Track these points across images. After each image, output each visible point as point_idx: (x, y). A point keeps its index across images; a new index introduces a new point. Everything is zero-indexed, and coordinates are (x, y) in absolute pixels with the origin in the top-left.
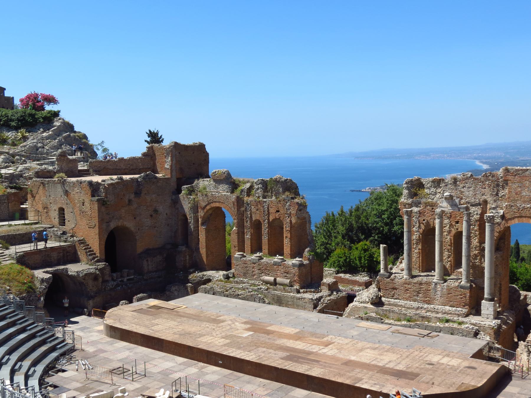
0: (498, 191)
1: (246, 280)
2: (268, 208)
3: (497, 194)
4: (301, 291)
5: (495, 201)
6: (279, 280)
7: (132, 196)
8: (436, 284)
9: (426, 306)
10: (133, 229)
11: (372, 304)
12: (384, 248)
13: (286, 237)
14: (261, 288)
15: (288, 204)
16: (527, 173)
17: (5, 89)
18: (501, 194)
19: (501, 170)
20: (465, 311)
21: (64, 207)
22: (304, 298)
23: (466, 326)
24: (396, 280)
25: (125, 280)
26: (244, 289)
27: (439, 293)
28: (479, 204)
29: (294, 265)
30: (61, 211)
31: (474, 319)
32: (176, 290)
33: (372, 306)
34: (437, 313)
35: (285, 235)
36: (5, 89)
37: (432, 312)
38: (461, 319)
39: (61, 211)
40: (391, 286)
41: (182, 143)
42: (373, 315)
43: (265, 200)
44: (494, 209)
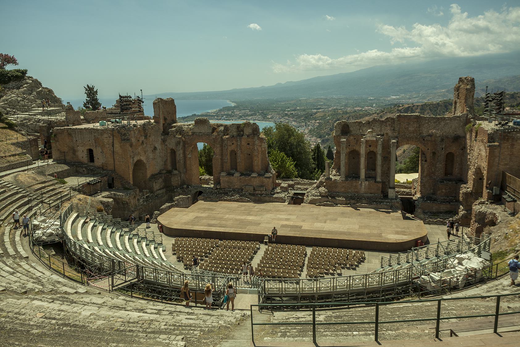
11: (322, 196)
30: (91, 152)
39: (91, 152)
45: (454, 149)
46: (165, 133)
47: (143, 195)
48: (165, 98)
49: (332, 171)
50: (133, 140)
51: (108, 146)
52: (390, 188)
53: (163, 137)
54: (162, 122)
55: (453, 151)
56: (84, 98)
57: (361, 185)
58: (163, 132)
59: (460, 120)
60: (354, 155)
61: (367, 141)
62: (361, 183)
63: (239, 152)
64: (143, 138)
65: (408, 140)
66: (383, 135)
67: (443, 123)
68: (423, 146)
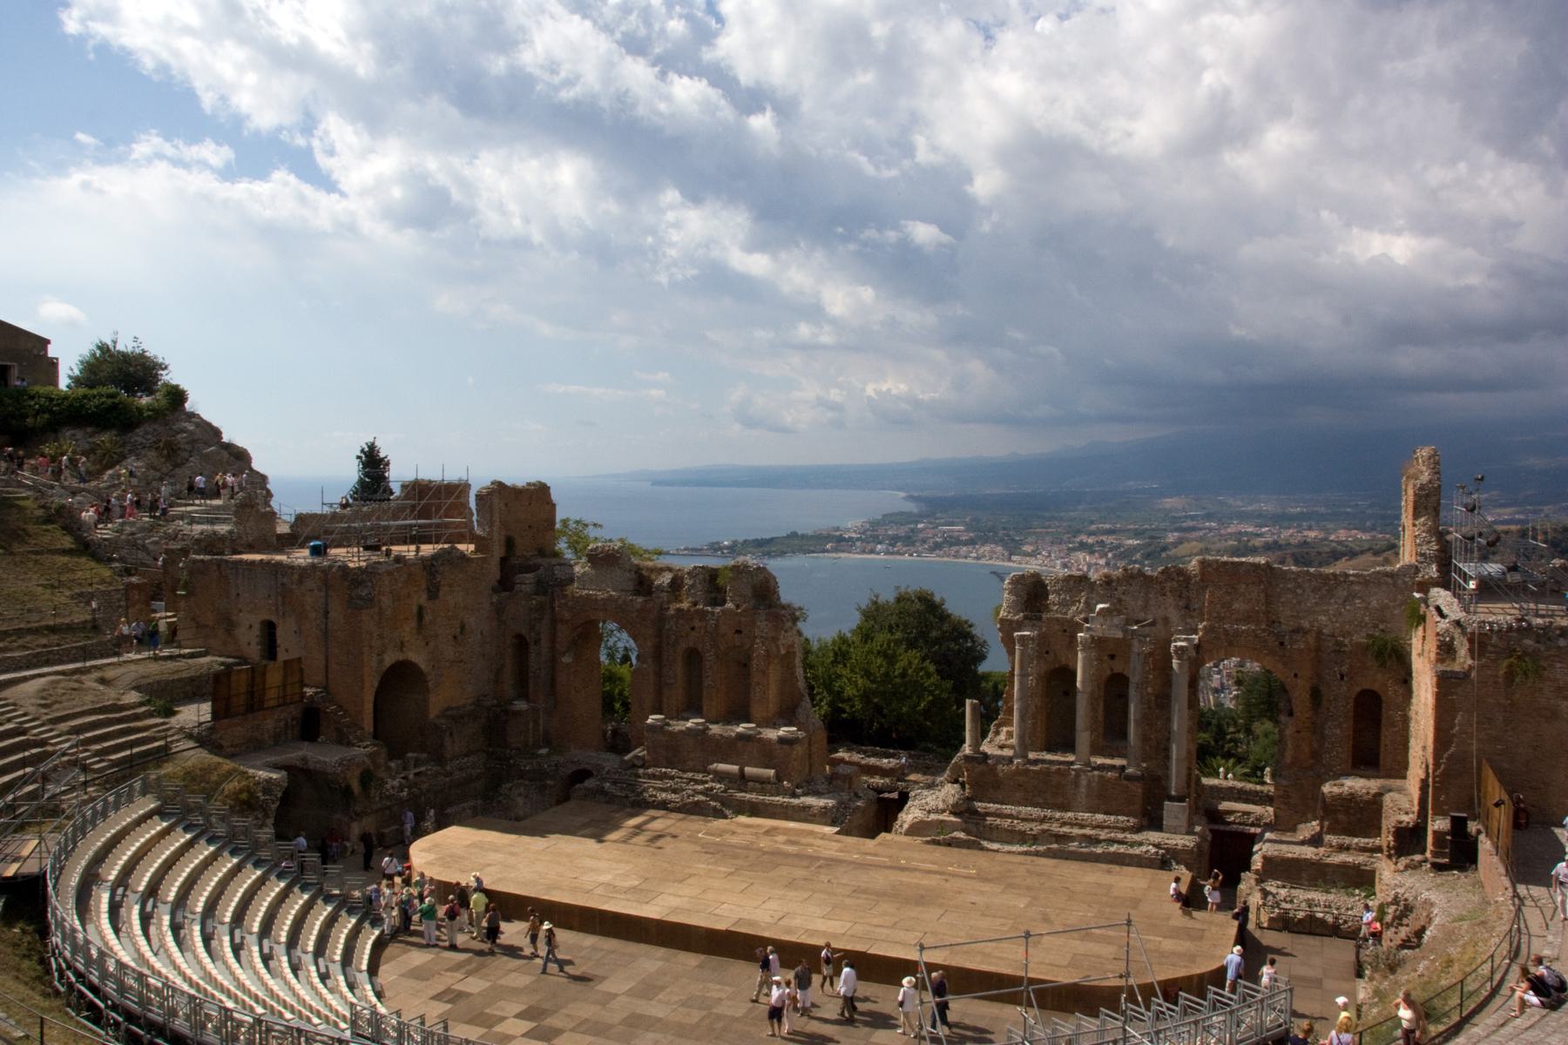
1: (674, 772)
3: (1187, 607)
4: (799, 791)
6: (748, 770)
7: (423, 599)
9: (1058, 815)
10: (423, 667)
12: (974, 707)
17: (48, 342)
19: (1194, 562)
21: (274, 619)
22: (810, 807)
23: (1144, 848)
26: (675, 791)
30: (269, 628)
31: (1154, 836)
33: (953, 819)
34: (1082, 827)
36: (48, 342)
37: (1072, 825)
38: (1130, 837)
39: (269, 628)
41: (508, 483)
42: (962, 835)
45: (1375, 679)
46: (505, 583)
47: (405, 768)
49: (997, 733)
50: (386, 601)
51: (313, 615)
52: (1171, 799)
54: (498, 551)
55: (1376, 687)
56: (350, 473)
57: (1076, 784)
58: (499, 582)
59: (1395, 585)
61: (1098, 643)
63: (709, 657)
64: (424, 596)
65: (1231, 644)
66: (1153, 624)
67: (1342, 593)
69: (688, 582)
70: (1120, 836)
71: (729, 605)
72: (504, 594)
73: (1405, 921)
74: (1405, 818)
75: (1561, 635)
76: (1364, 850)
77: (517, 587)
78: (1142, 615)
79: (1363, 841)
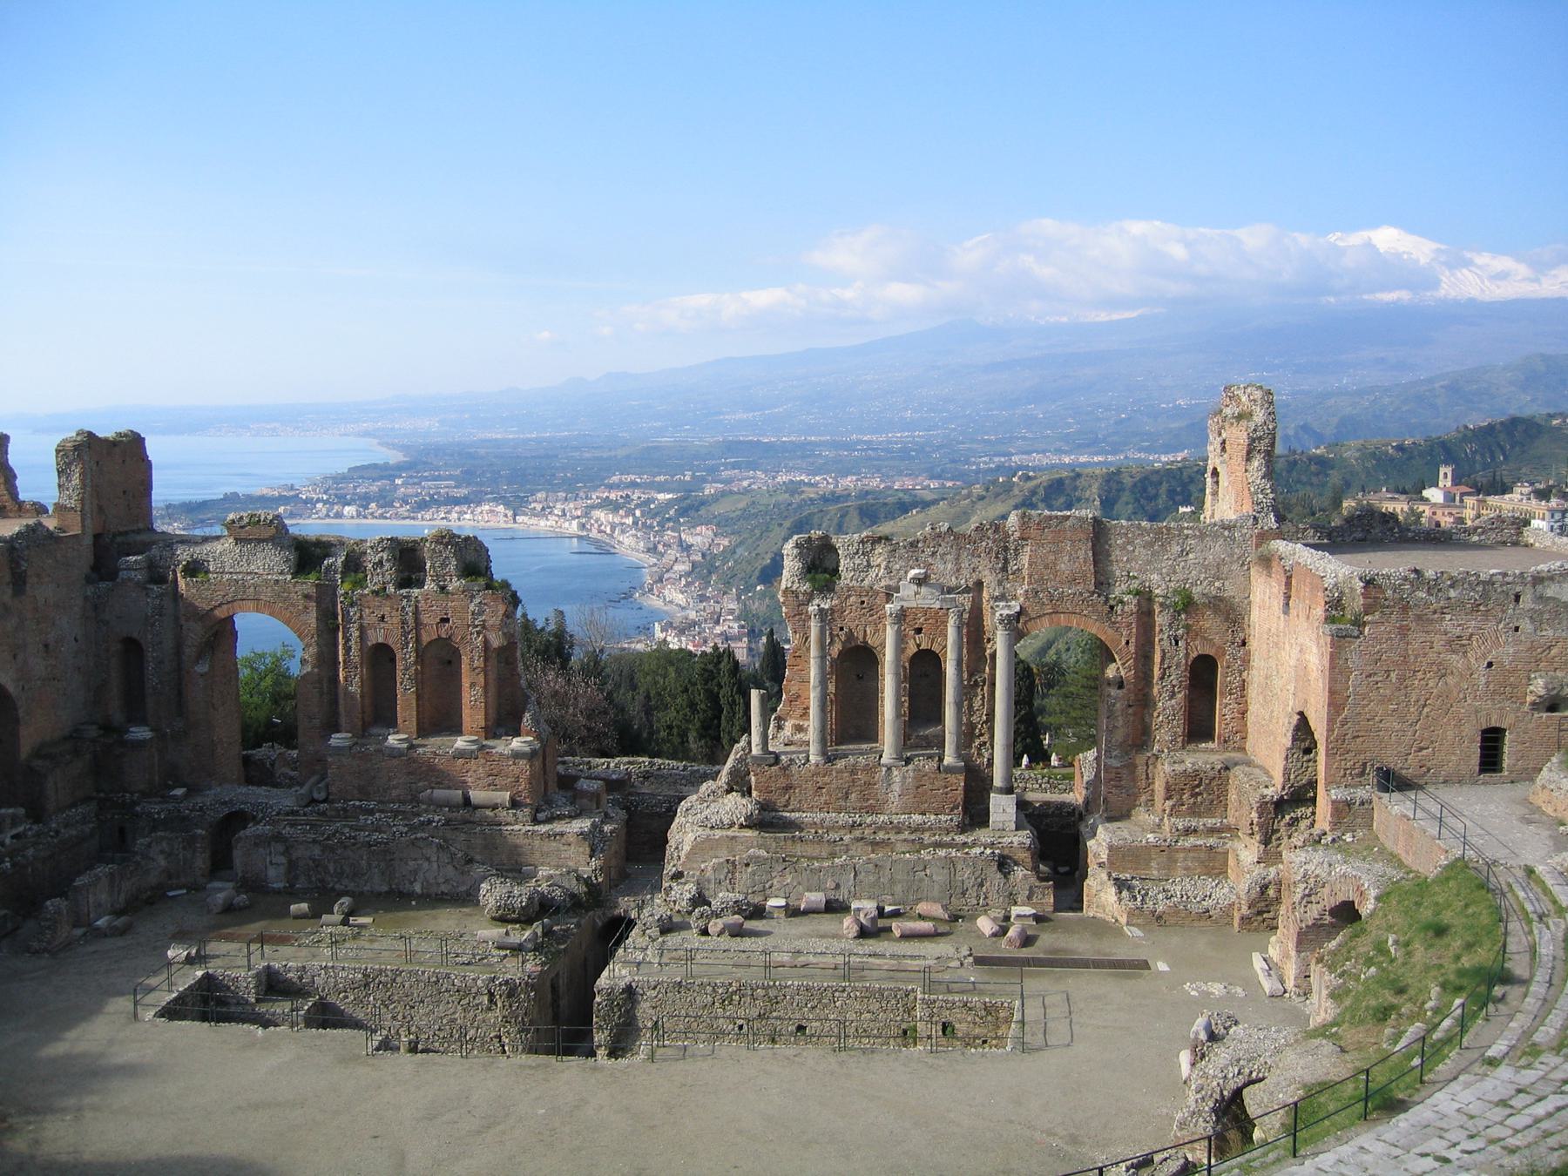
0: (1006, 561)
2: (416, 613)
3: (1004, 569)
5: (1000, 583)
8: (889, 769)
10: (11, 688)
13: (473, 685)
14: (430, 822)
15: (477, 601)
16: (1068, 523)
18: (1012, 567)
20: (957, 817)
24: (794, 768)
25: (8, 841)
26: (378, 830)
27: (896, 788)
28: (967, 590)
29: (516, 755)
31: (983, 835)
32: (162, 852)
35: (466, 683)
38: (960, 839)
40: (782, 782)
43: (403, 591)
44: (1002, 597)
48: (105, 431)
53: (90, 590)
60: (855, 664)
62: (889, 769)
68: (1110, 631)
69: (371, 558)
70: (947, 839)
71: (430, 585)
72: (103, 585)
73: (1313, 898)
74: (1269, 792)
75: (1452, 586)
76: (1212, 831)
77: (123, 575)
78: (954, 582)
79: (1210, 822)
